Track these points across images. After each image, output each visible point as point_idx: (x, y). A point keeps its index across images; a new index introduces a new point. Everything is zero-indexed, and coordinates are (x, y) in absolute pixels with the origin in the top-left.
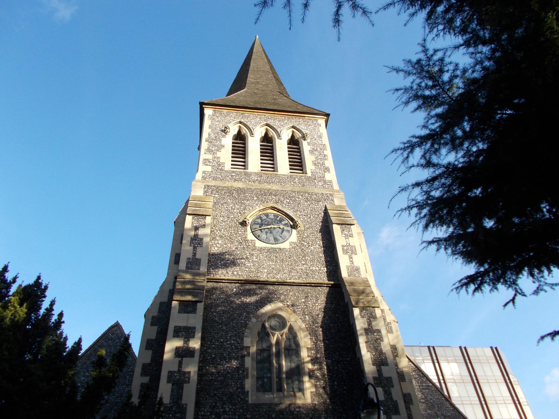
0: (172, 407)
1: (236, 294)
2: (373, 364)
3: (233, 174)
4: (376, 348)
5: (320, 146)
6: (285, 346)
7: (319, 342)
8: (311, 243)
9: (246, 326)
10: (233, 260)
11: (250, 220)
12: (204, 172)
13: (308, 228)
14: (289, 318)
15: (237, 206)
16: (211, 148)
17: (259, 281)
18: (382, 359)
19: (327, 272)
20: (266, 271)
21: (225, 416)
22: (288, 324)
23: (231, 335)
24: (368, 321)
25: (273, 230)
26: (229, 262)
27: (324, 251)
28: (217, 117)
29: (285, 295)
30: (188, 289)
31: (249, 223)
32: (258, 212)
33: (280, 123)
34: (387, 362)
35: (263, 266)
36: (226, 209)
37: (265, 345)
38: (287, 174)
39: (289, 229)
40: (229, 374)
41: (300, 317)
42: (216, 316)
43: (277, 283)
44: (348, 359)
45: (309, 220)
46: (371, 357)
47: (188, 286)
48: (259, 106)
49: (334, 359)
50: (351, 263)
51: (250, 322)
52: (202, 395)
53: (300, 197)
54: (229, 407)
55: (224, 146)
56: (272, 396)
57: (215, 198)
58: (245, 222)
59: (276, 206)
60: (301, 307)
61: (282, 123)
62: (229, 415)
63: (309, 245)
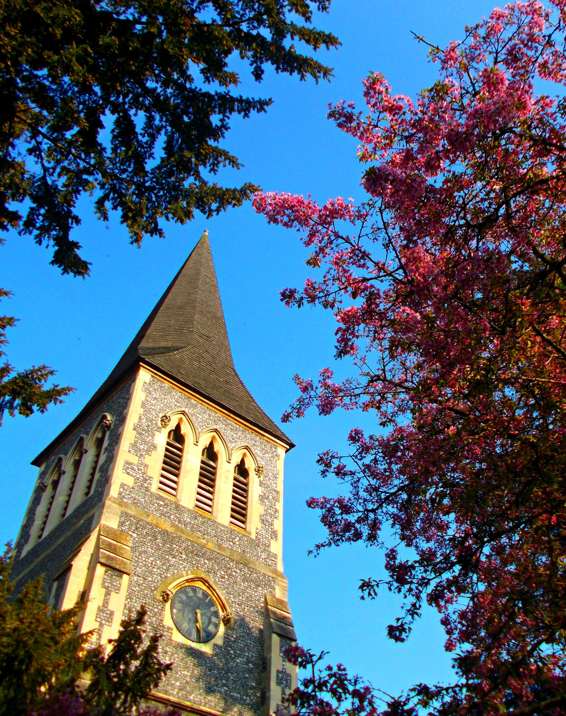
3: (161, 503)
12: (123, 485)
15: (158, 562)
59: (207, 578)
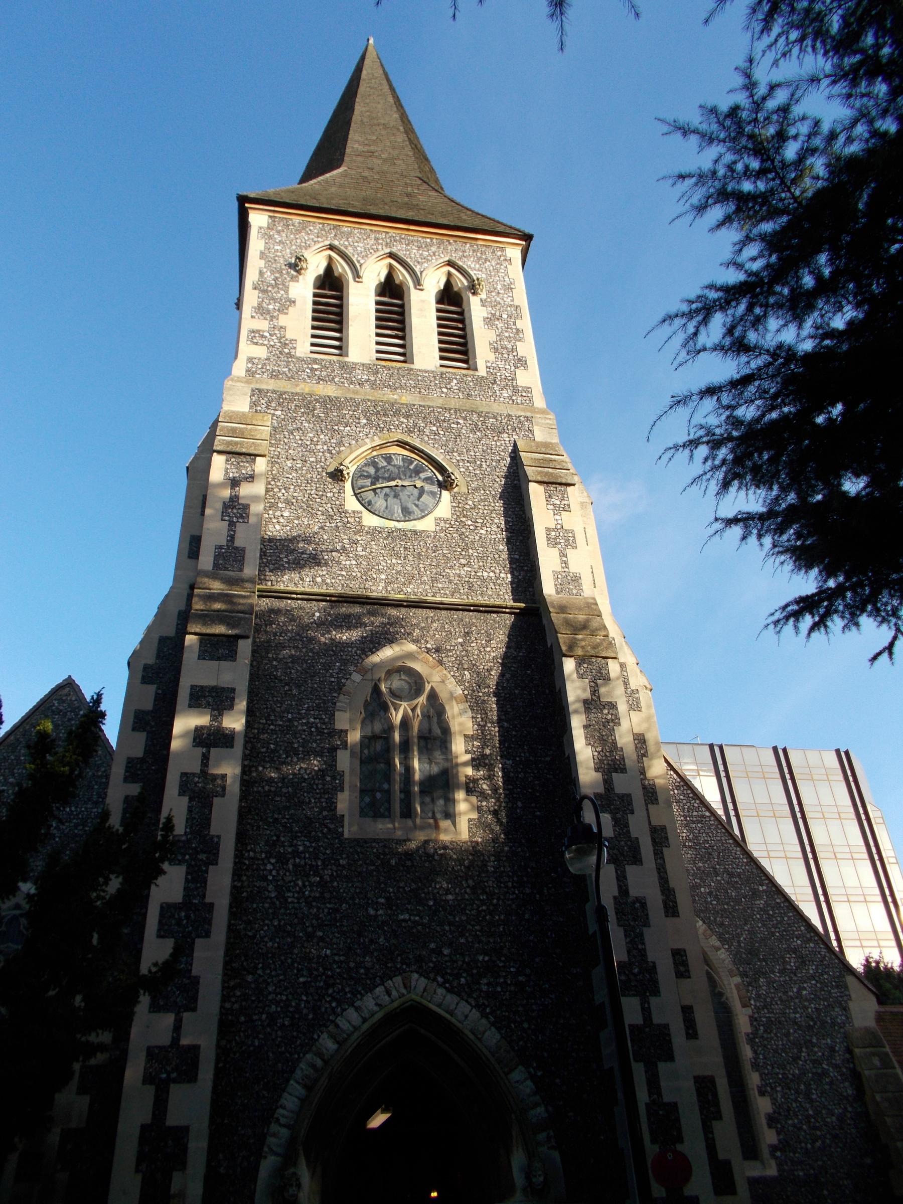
0: (189, 841)
1: (321, 624)
2: (597, 770)
3: (316, 366)
4: (605, 738)
5: (509, 309)
6: (419, 731)
7: (489, 725)
8: (482, 521)
9: (341, 689)
10: (313, 552)
11: (350, 468)
12: (250, 360)
13: (476, 489)
14: (431, 675)
15: (322, 436)
16: (264, 305)
17: (368, 598)
18: (614, 760)
19: (512, 583)
20: (383, 577)
21: (297, 860)
22: (428, 688)
23: (308, 707)
24: (593, 684)
25: (402, 491)
26: (305, 556)
27: (508, 538)
28: (279, 232)
29: (422, 629)
30: (218, 611)
31: (348, 474)
32: (370, 451)
33: (421, 252)
34: (624, 765)
35: (377, 567)
36: (300, 442)
37: (378, 727)
38: (433, 369)
39: (435, 488)
40: (304, 782)
41: (452, 673)
42: (278, 667)
43: (405, 604)
44: (548, 759)
45: (478, 472)
46: (593, 756)
47: (218, 606)
48: (373, 210)
49: (518, 759)
50: (564, 565)
51: (349, 681)
52: (249, 821)
53: (461, 421)
54: (304, 844)
55: (294, 302)
56: (390, 826)
57: (275, 418)
58: (341, 471)
59: (408, 440)
60: (456, 653)
61: (426, 253)
62: (305, 858)
63: (477, 524)
